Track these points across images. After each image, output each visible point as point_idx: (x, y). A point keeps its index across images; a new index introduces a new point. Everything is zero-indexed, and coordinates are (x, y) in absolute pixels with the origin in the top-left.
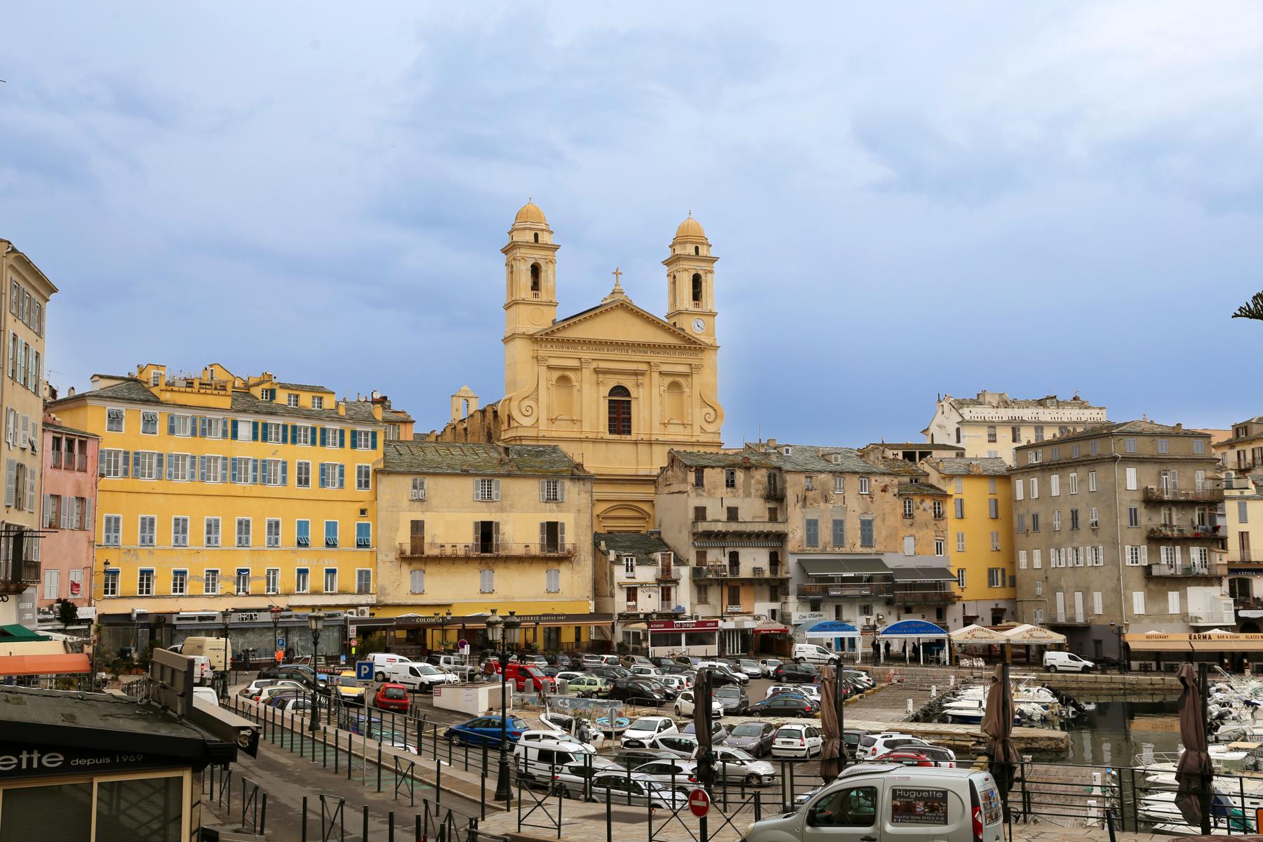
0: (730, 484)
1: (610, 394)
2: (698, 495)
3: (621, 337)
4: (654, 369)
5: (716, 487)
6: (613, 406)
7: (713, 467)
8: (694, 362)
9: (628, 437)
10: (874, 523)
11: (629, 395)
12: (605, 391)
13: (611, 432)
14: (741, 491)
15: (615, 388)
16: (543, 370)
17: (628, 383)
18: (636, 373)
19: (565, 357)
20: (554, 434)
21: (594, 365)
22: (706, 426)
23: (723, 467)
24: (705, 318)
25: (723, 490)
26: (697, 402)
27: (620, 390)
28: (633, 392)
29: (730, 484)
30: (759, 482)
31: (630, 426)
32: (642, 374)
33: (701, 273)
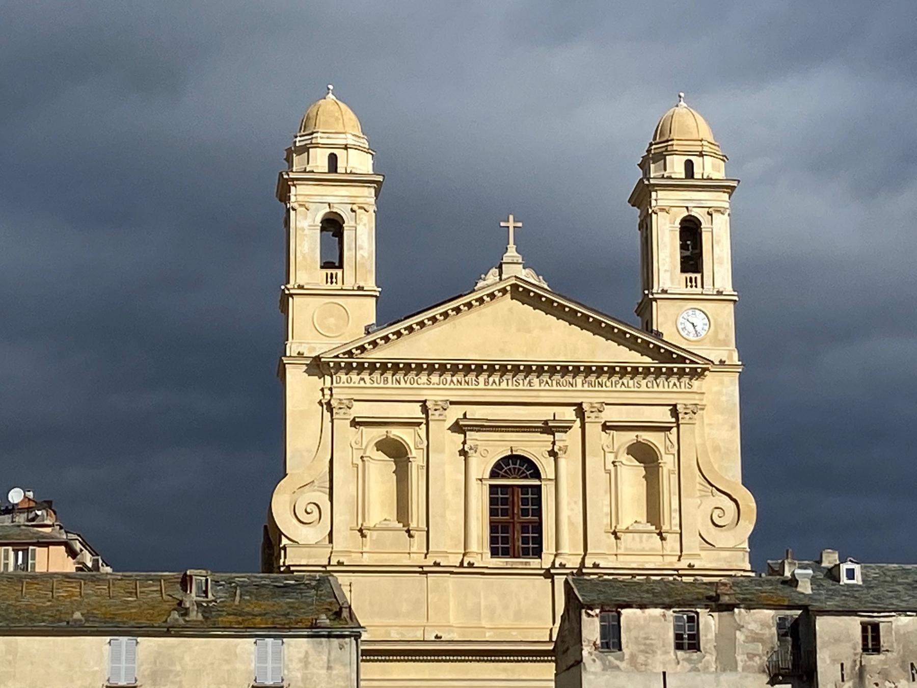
0: (687, 640)
1: (494, 474)
2: (607, 667)
3: (517, 354)
4: (590, 417)
5: (649, 650)
6: (499, 500)
7: (642, 607)
8: (680, 401)
9: (534, 562)
10: (734, 673)
11: (537, 475)
12: (481, 466)
13: (494, 553)
14: (710, 658)
15: (506, 459)
16: (342, 425)
17: (533, 447)
18: (547, 428)
19: (394, 400)
20: (366, 559)
21: (455, 413)
22: (712, 534)
23: (668, 607)
24: (708, 307)
25: (666, 656)
26: (693, 482)
27: (516, 464)
28: (546, 467)
29: (687, 640)
30: (755, 638)
31: (539, 541)
32: (565, 429)
33: (695, 213)
